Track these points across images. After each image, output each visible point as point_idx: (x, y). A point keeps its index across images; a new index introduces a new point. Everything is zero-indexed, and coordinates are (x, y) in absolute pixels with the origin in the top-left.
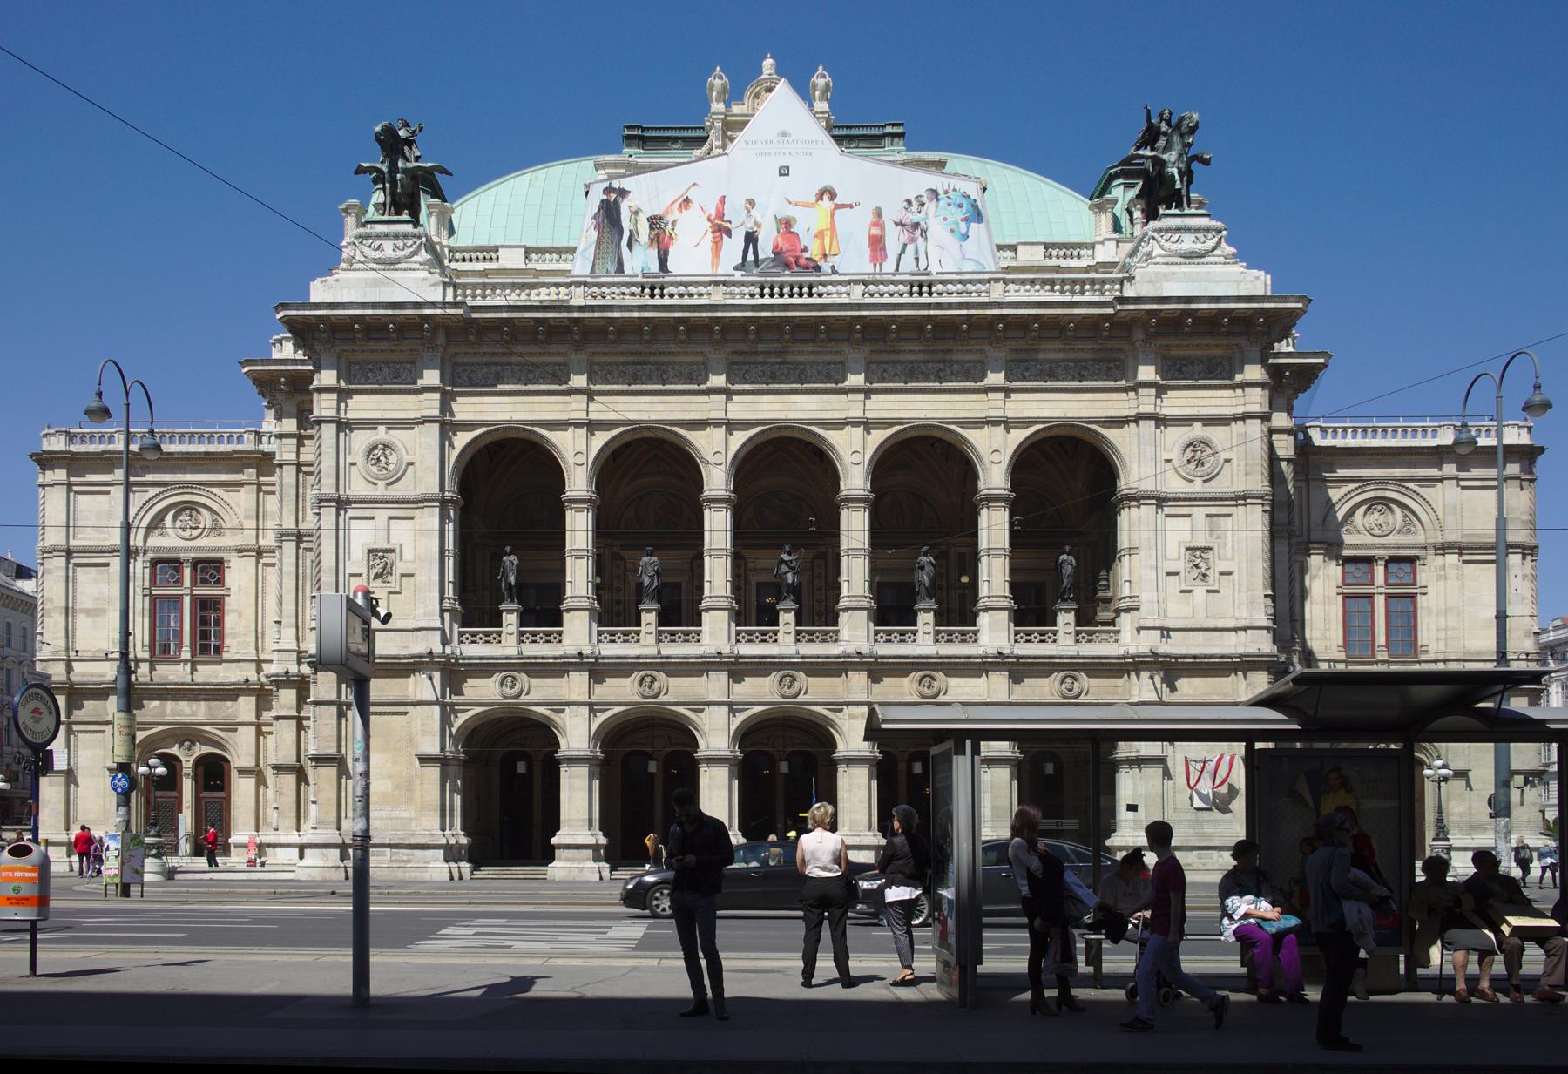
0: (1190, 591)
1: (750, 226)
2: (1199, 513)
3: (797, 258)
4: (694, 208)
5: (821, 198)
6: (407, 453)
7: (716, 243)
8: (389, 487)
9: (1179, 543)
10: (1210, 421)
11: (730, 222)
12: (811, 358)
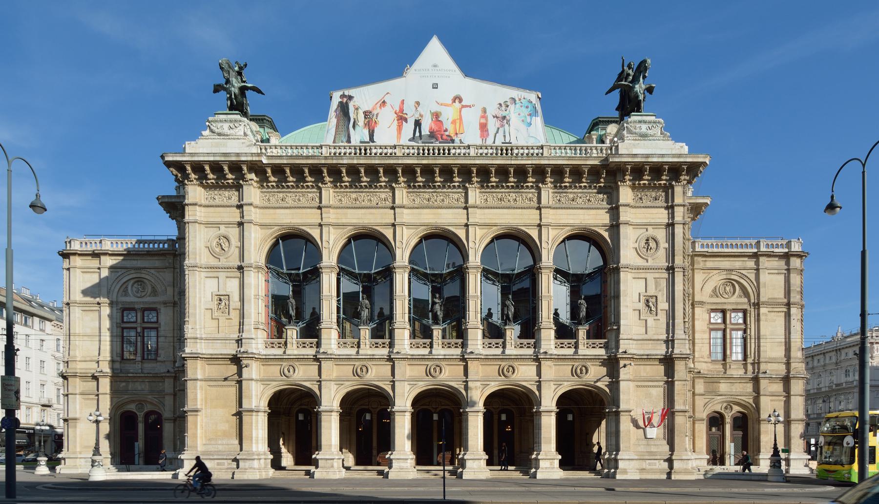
1: (417, 116)
3: (442, 135)
4: (388, 106)
5: (454, 101)
7: (399, 126)
11: (407, 114)
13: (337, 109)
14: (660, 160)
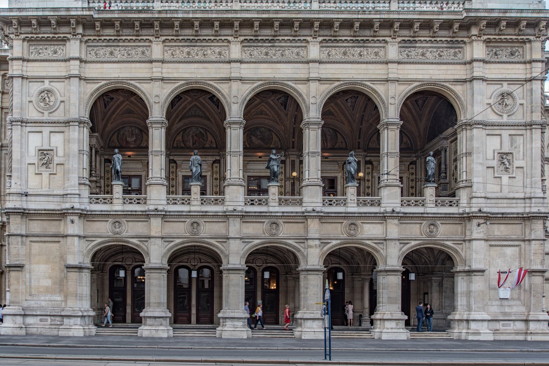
0: (500, 178)
2: (505, 133)
6: (61, 96)
8: (51, 115)
9: (494, 151)
10: (512, 81)
12: (289, 44)
14: (519, 15)
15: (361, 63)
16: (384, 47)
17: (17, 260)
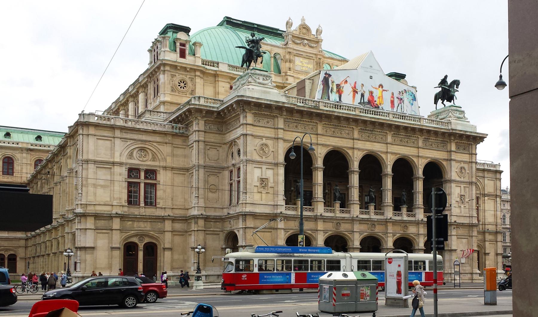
13: (323, 80)
15: (408, 147)
16: (416, 140)
17: (250, 243)
